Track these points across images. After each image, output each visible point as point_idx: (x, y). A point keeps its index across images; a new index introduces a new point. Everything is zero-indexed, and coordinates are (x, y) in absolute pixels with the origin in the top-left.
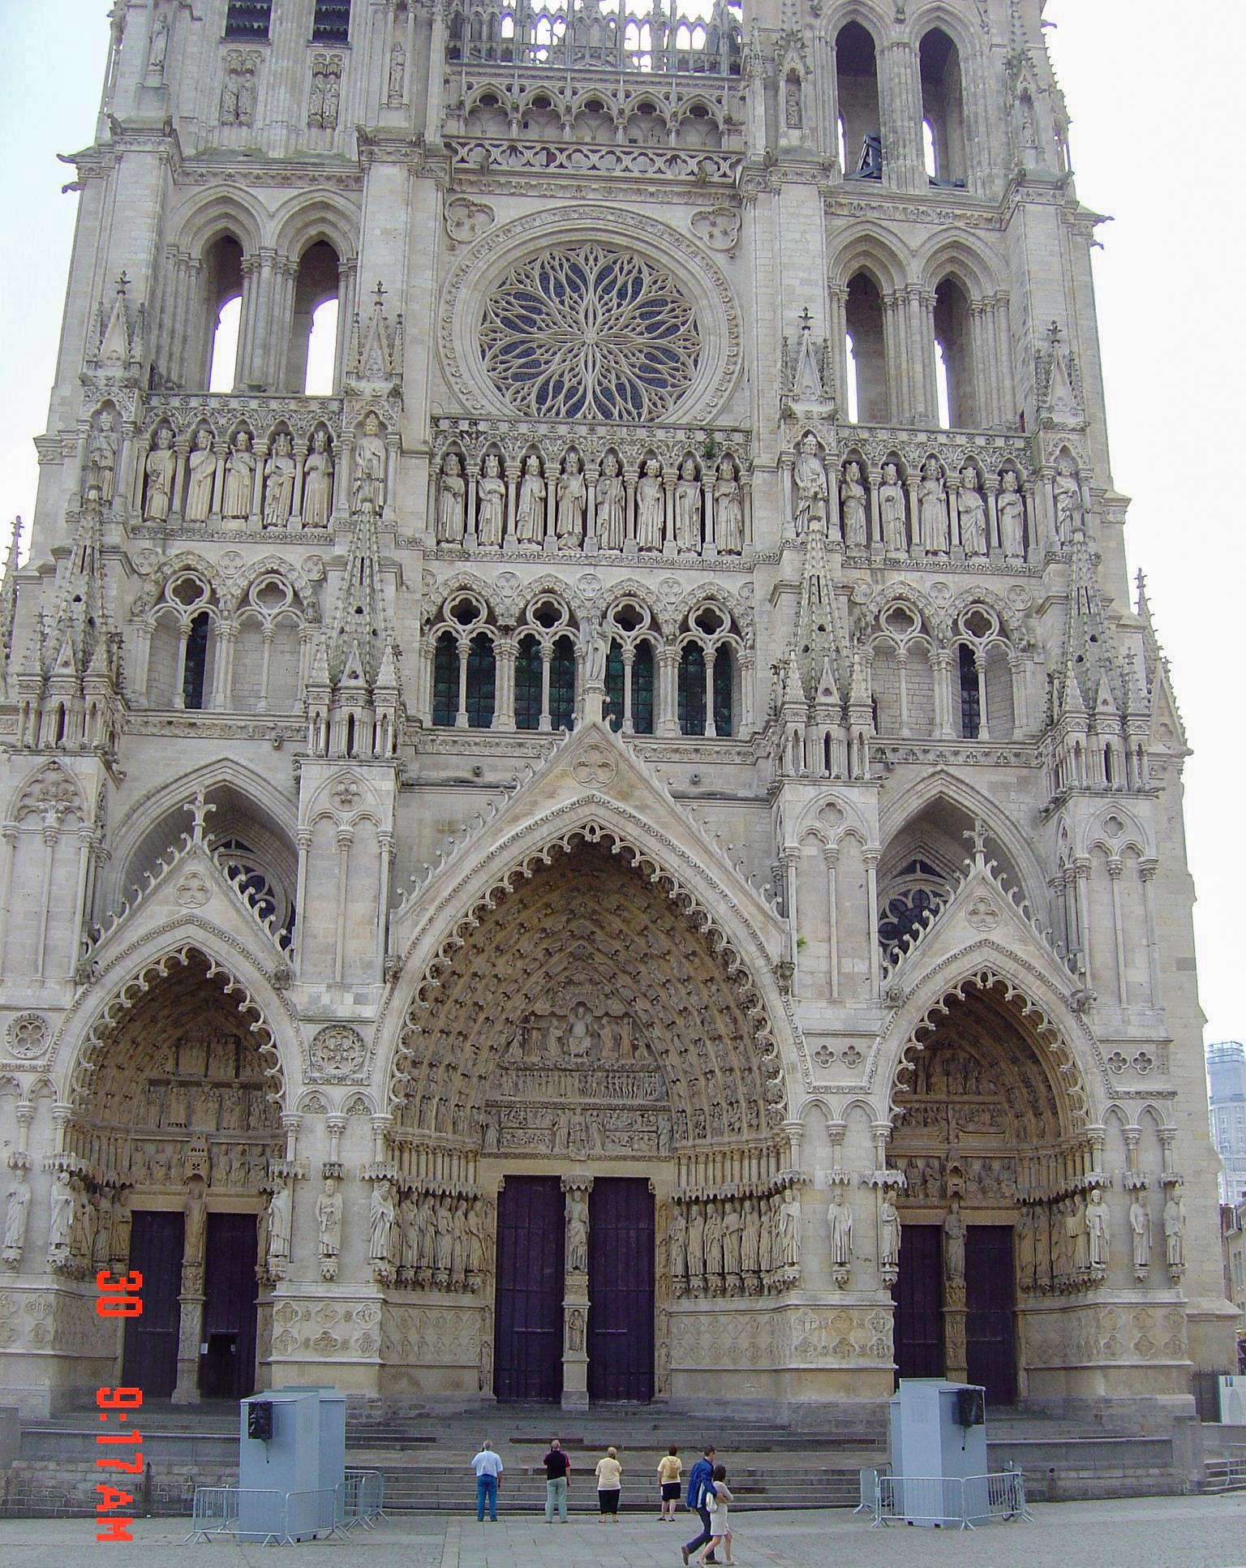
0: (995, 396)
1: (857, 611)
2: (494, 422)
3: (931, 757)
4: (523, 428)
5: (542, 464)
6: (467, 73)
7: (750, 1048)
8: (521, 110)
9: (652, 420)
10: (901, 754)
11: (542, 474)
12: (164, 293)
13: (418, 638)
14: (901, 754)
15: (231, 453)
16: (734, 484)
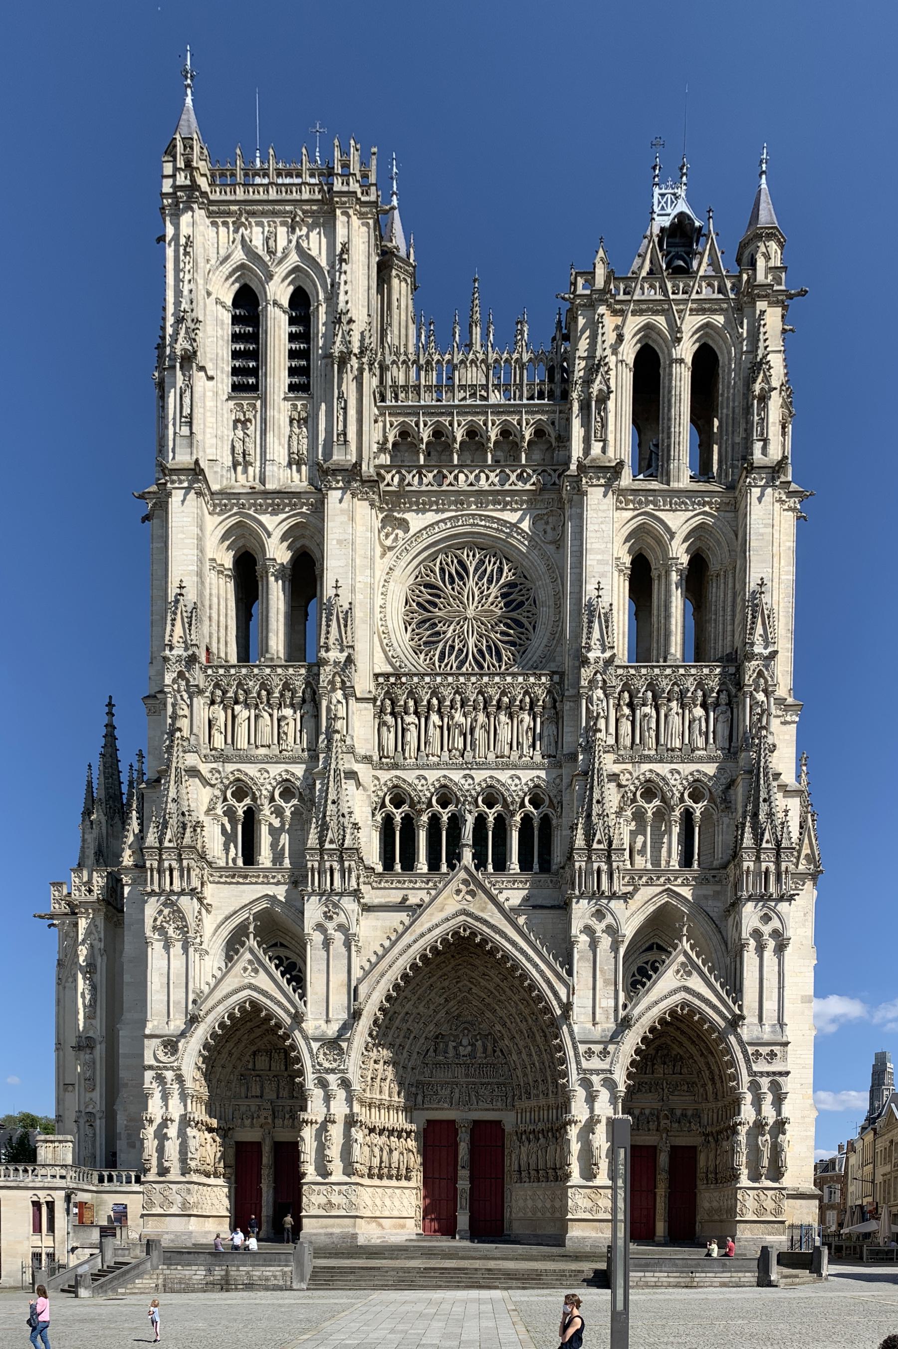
0: (721, 638)
1: (622, 790)
2: (411, 675)
3: (662, 880)
4: (427, 679)
5: (439, 702)
6: (389, 414)
7: (553, 1050)
8: (425, 440)
9: (507, 669)
10: (644, 879)
11: (439, 709)
12: (211, 595)
13: (370, 818)
14: (644, 879)
15: (257, 704)
16: (553, 711)
